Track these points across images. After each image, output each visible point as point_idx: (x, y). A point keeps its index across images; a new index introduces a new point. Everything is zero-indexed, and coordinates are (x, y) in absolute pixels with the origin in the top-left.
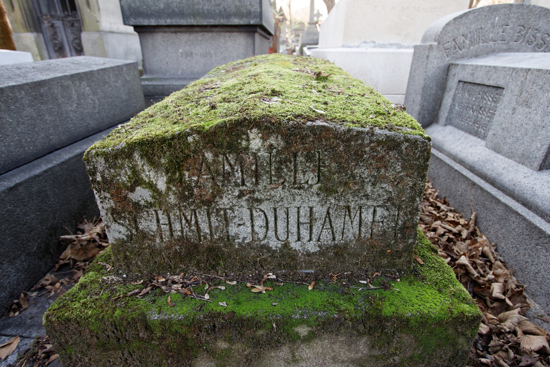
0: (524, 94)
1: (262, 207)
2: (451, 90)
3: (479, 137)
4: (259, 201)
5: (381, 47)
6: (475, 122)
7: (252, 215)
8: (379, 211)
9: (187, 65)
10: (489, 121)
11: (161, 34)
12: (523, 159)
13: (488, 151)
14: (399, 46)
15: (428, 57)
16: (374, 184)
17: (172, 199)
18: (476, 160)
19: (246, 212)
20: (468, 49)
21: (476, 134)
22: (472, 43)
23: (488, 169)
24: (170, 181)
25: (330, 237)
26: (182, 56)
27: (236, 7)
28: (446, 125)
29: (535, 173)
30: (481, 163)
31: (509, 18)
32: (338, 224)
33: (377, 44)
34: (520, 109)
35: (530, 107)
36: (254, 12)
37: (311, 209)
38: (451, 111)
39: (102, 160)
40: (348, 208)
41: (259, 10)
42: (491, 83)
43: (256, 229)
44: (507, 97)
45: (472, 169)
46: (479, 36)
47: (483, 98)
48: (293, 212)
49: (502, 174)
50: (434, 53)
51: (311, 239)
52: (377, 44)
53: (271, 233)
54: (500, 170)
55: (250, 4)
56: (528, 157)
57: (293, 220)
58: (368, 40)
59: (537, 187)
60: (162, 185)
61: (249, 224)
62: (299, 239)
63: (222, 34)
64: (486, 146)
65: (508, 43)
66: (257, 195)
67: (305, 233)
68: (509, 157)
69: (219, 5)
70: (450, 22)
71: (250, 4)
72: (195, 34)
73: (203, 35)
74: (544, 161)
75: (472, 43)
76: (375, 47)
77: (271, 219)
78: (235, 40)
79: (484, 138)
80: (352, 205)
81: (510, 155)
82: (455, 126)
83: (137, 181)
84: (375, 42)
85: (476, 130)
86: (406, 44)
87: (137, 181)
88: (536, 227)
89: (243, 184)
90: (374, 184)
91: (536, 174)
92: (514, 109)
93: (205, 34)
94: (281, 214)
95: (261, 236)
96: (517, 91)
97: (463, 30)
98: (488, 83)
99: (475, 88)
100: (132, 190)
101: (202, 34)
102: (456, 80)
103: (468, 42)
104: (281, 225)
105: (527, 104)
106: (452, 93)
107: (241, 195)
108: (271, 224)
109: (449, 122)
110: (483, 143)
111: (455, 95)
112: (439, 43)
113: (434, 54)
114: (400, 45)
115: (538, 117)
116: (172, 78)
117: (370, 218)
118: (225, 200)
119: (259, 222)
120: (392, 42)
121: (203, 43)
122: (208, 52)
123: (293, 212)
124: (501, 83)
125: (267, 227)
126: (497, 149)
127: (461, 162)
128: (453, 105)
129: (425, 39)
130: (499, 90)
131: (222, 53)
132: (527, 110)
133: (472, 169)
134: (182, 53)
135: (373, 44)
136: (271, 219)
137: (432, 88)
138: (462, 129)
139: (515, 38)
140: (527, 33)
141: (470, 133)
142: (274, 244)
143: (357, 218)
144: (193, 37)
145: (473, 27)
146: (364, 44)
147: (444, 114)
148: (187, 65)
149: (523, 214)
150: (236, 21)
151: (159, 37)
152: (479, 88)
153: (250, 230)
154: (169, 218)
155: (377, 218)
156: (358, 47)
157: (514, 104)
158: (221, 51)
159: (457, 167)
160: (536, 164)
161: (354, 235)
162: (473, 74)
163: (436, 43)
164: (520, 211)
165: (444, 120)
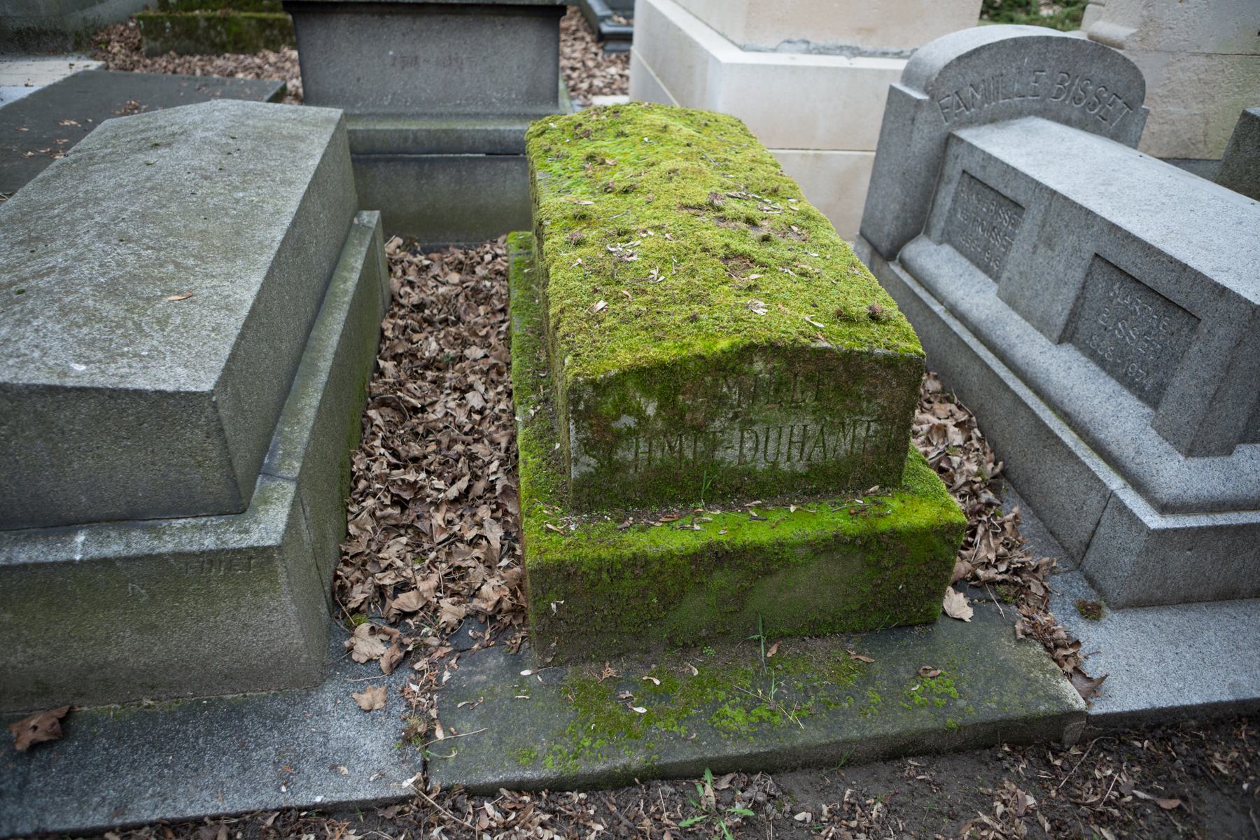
0: (1048, 229)
1: (755, 428)
2: (950, 181)
3: (990, 276)
4: (752, 423)
5: (820, 53)
6: (985, 249)
7: (742, 436)
8: (873, 426)
9: (405, 84)
10: (1005, 254)
11: (347, 16)
12: (1042, 325)
13: (1001, 304)
14: (856, 52)
15: (913, 120)
16: (869, 402)
17: (660, 425)
18: (984, 317)
19: (737, 433)
20: (980, 108)
21: (986, 270)
22: (986, 99)
23: (997, 336)
24: (660, 407)
25: (821, 455)
26: (393, 65)
28: (941, 243)
29: (1054, 347)
30: (990, 325)
31: (1045, 60)
32: (831, 441)
33: (812, 46)
34: (1042, 249)
35: (1053, 250)
37: (805, 426)
38: (949, 221)
39: (590, 389)
40: (843, 424)
43: (745, 451)
44: (1029, 224)
45: (976, 332)
46: (997, 88)
47: (997, 212)
48: (786, 431)
49: (1015, 345)
50: (924, 114)
51: (801, 458)
52: (812, 46)
53: (760, 455)
54: (1014, 340)
56: (1048, 323)
57: (784, 440)
58: (795, 38)
59: (1053, 369)
60: (651, 410)
61: (737, 447)
62: (789, 459)
63: (487, 19)
64: (999, 295)
65: (1043, 100)
66: (752, 416)
67: (795, 452)
68: (1027, 319)
70: (951, 62)
72: (426, 19)
73: (445, 21)
74: (1064, 331)
75: (986, 99)
76: (809, 52)
77: (762, 439)
78: (515, 32)
79: (996, 278)
80: (847, 421)
81: (1027, 316)
82: (957, 248)
83: (624, 407)
84: (808, 42)
85: (988, 264)
87: (624, 407)
88: (1045, 425)
89: (739, 406)
90: (869, 402)
91: (1055, 350)
92: (1035, 247)
93: (450, 18)
94: (773, 434)
95: (749, 459)
96: (1039, 217)
97: (972, 76)
98: (1003, 191)
99: (987, 191)
100: (617, 418)
101: (442, 17)
102: (959, 168)
103: (979, 97)
104: (771, 445)
106: (952, 187)
107: (736, 416)
108: (761, 446)
109: (947, 238)
110: (995, 287)
111: (957, 194)
112: (932, 97)
113: (922, 115)
114: (858, 48)
115: (1061, 268)
116: (370, 114)
117: (864, 434)
118: (717, 423)
119: (749, 444)
120: (842, 42)
121: (443, 36)
122: (454, 56)
123: (786, 431)
124: (1021, 199)
125: (756, 449)
126: (1011, 302)
127: (962, 318)
128: (953, 211)
129: (908, 77)
130: (1019, 210)
132: (1050, 252)
133: (976, 332)
134: (394, 58)
135: (804, 46)
136: (762, 439)
137: (919, 174)
138: (966, 256)
139: (1055, 92)
140: (1072, 84)
141: (978, 266)
142: (761, 466)
143: (851, 434)
144: (420, 23)
145: (989, 72)
146: (787, 46)
147: (939, 223)
148: (405, 84)
149: (1033, 407)
151: (342, 21)
153: (737, 453)
154: (650, 444)
155: (871, 433)
156: (774, 50)
157: (1034, 239)
158: (485, 54)
159: (956, 326)
160: (1055, 335)
161: (846, 451)
162: (984, 167)
163: (926, 98)
164: (1030, 403)
165: (939, 233)
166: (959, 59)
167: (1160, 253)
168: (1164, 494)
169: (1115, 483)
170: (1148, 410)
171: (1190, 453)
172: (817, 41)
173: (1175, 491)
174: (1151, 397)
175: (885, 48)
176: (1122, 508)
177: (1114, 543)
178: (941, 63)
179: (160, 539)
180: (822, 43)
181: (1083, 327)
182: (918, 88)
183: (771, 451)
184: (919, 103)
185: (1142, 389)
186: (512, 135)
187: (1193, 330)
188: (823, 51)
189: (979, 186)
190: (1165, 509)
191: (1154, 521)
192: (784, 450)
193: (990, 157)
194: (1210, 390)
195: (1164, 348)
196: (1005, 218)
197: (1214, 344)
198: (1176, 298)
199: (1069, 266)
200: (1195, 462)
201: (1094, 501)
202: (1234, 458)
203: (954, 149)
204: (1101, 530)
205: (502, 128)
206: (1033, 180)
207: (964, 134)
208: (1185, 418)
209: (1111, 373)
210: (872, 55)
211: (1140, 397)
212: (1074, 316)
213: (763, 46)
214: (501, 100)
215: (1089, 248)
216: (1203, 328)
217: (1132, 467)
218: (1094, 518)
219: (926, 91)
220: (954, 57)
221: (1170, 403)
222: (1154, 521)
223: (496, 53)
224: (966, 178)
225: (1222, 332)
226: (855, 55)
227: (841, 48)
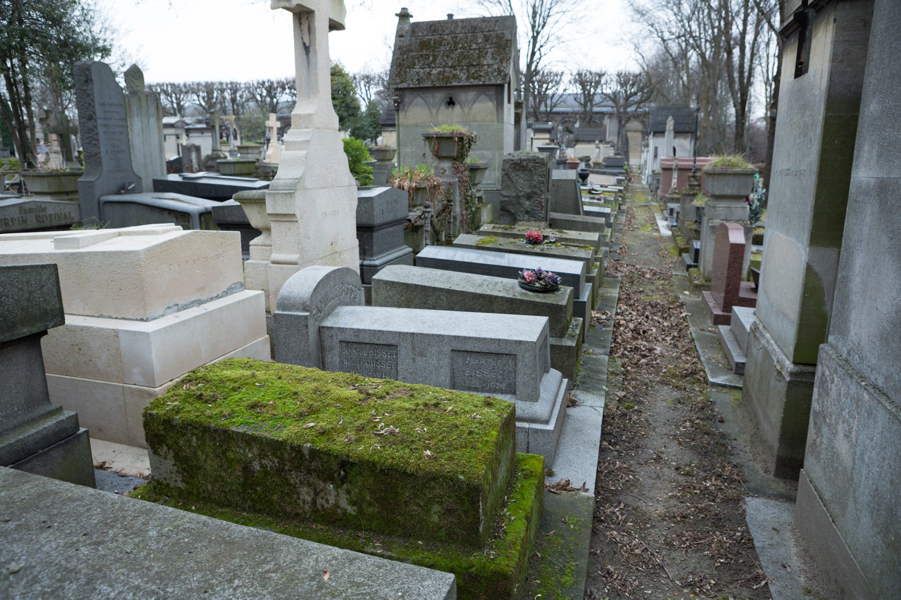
2: (332, 349)
14: (200, 302)
34: (418, 359)
36: (51, 310)
41: (58, 305)
42: (382, 342)
55: (45, 301)
58: (171, 305)
71: (45, 301)
76: (179, 310)
86: (204, 298)
97: (320, 297)
98: (378, 342)
102: (336, 341)
105: (422, 354)
106: (336, 351)
115: (435, 362)
124: (393, 342)
135: (176, 308)
146: (168, 311)
152: (368, 346)
156: (163, 316)
167: (485, 339)
169: (526, 425)
172: (181, 303)
176: (536, 431)
181: (458, 381)
182: (298, 310)
184: (306, 318)
185: (501, 390)
186: (31, 439)
188: (185, 307)
189: (355, 345)
190: (547, 422)
191: (551, 427)
193: (359, 330)
196: (384, 355)
197: (527, 360)
198: (503, 351)
199: (439, 360)
203: (326, 334)
204: (531, 445)
205: (21, 437)
206: (396, 332)
207: (328, 323)
208: (530, 390)
212: (453, 377)
213: (156, 315)
215: (447, 349)
216: (519, 357)
217: (526, 416)
218: (526, 442)
224: (344, 344)
225: (527, 355)
226: (200, 304)
227: (193, 302)
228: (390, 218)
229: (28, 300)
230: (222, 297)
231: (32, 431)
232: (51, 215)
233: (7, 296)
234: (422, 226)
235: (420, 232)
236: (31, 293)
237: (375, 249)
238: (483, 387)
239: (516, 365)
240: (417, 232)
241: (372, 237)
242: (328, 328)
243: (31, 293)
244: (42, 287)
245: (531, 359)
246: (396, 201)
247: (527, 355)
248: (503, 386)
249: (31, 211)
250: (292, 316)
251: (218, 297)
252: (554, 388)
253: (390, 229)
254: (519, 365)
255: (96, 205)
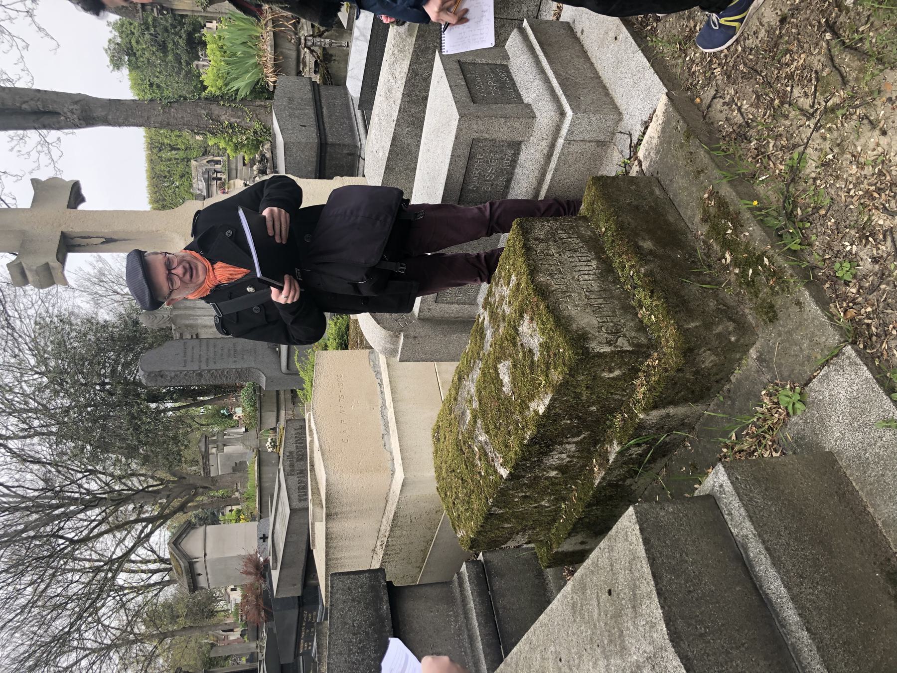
27: (367, 608)
36: (370, 581)
38: (464, 303)
48: (573, 264)
55: (361, 587)
67: (584, 259)
69: (367, 633)
71: (361, 587)
86: (380, 401)
94: (578, 268)
111: (448, 303)
131: (430, 637)
135: (386, 437)
150: (385, 607)
156: (391, 453)
166: (379, 323)
168: (556, 118)
169: (561, 141)
170: (523, 147)
171: (534, 117)
173: (553, 113)
174: (516, 146)
175: (379, 393)
176: (570, 132)
177: (589, 129)
178: (383, 331)
179: (747, 536)
180: (382, 427)
183: (588, 268)
186: (478, 607)
187: (478, 140)
188: (387, 426)
190: (562, 114)
191: (569, 113)
192: (584, 264)
194: (502, 121)
195: (491, 151)
197: (482, 128)
200: (538, 114)
201: (574, 148)
202: (531, 102)
203: (427, 314)
209: (512, 174)
210: (383, 399)
211: (519, 154)
214: (456, 621)
219: (397, 337)
220: (379, 326)
221: (516, 137)
222: (569, 113)
223: (425, 629)
225: (475, 127)
228: (310, 111)
229: (359, 602)
230: (381, 380)
231: (472, 605)
232: (297, 447)
233: (354, 621)
234: (324, 49)
235: (331, 52)
236: (353, 600)
237: (347, 141)
238: (507, 173)
239: (486, 139)
240: (331, 56)
241: (333, 145)
242: (420, 311)
243: (353, 600)
244: (349, 589)
245: (480, 122)
246: (291, 100)
247: (475, 127)
248: (510, 152)
249: (292, 465)
250: (403, 348)
251: (381, 385)
252: (529, 64)
253: (325, 110)
254: (487, 136)
255: (290, 376)
